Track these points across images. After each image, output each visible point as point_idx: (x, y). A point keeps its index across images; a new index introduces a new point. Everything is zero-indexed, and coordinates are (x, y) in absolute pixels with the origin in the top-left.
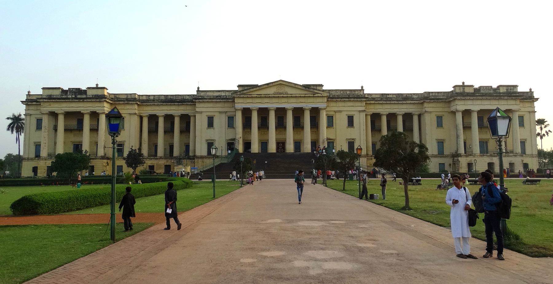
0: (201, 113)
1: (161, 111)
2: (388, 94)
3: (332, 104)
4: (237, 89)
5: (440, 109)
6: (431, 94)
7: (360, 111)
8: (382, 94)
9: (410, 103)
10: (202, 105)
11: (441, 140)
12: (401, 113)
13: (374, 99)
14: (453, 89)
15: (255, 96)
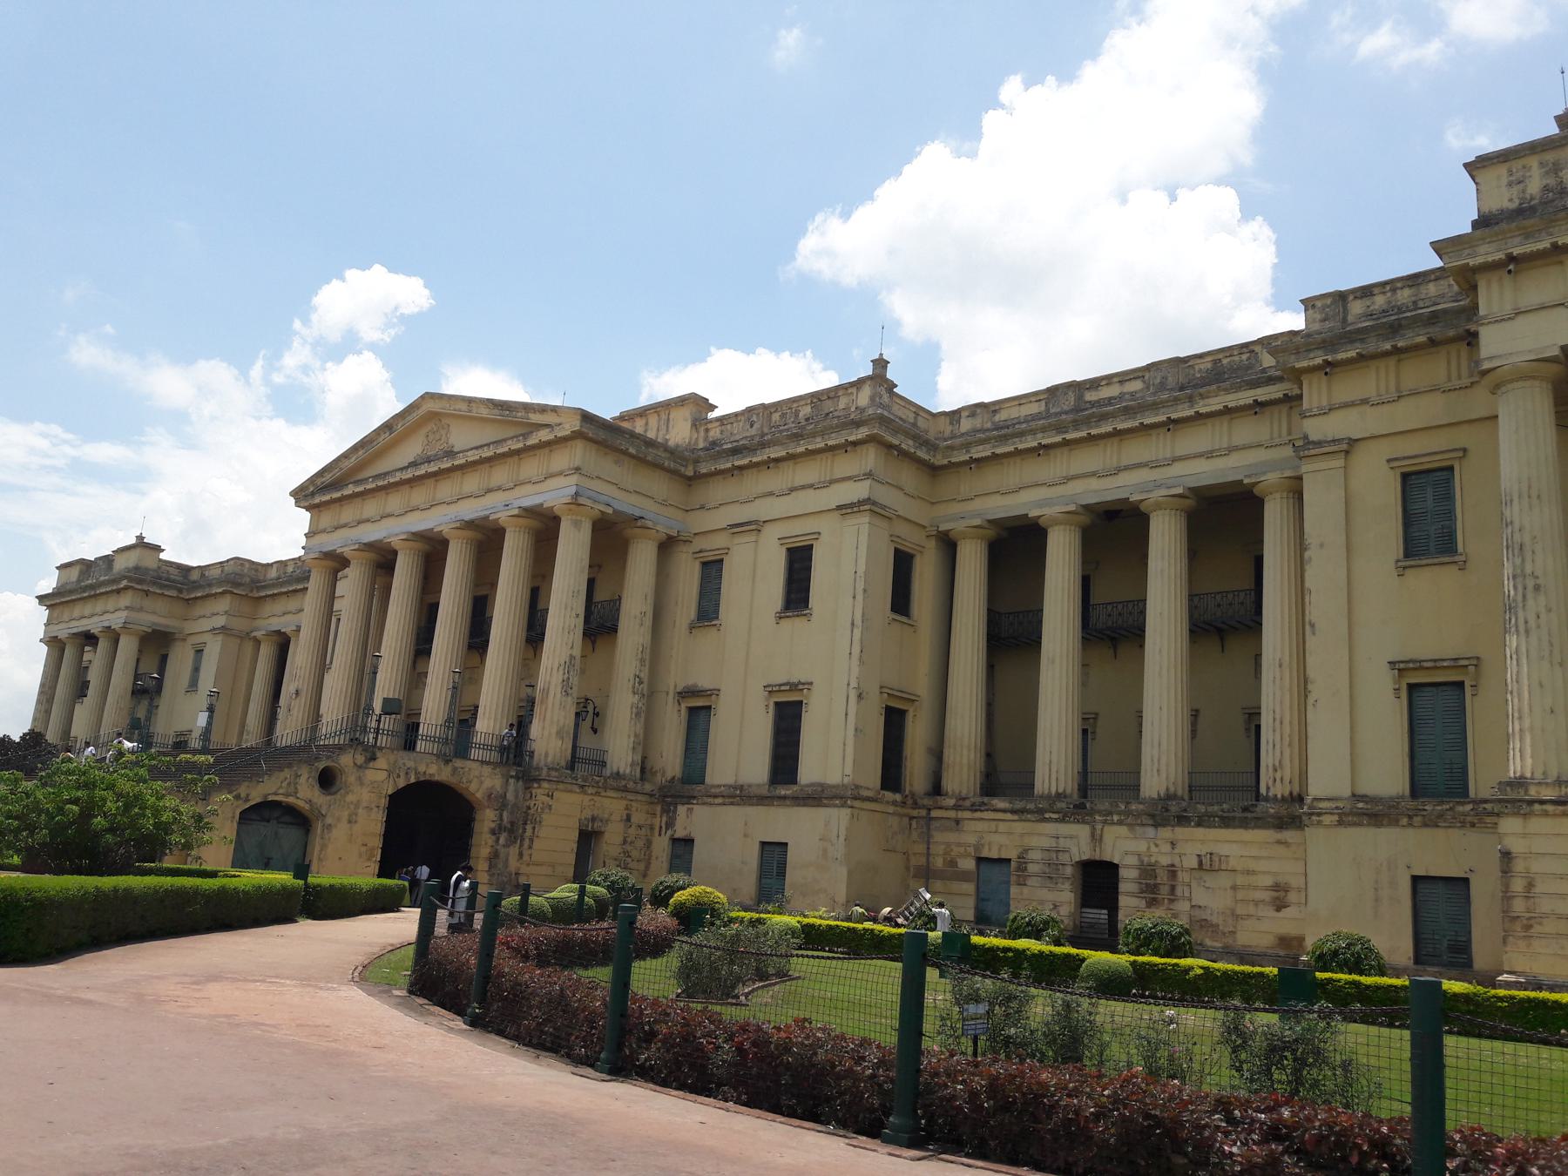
2: (1094, 384)
3: (718, 491)
5: (1429, 409)
6: (1357, 308)
7: (845, 509)
8: (1053, 391)
9: (1227, 411)
11: (1436, 665)
12: (1157, 495)
13: (1007, 431)
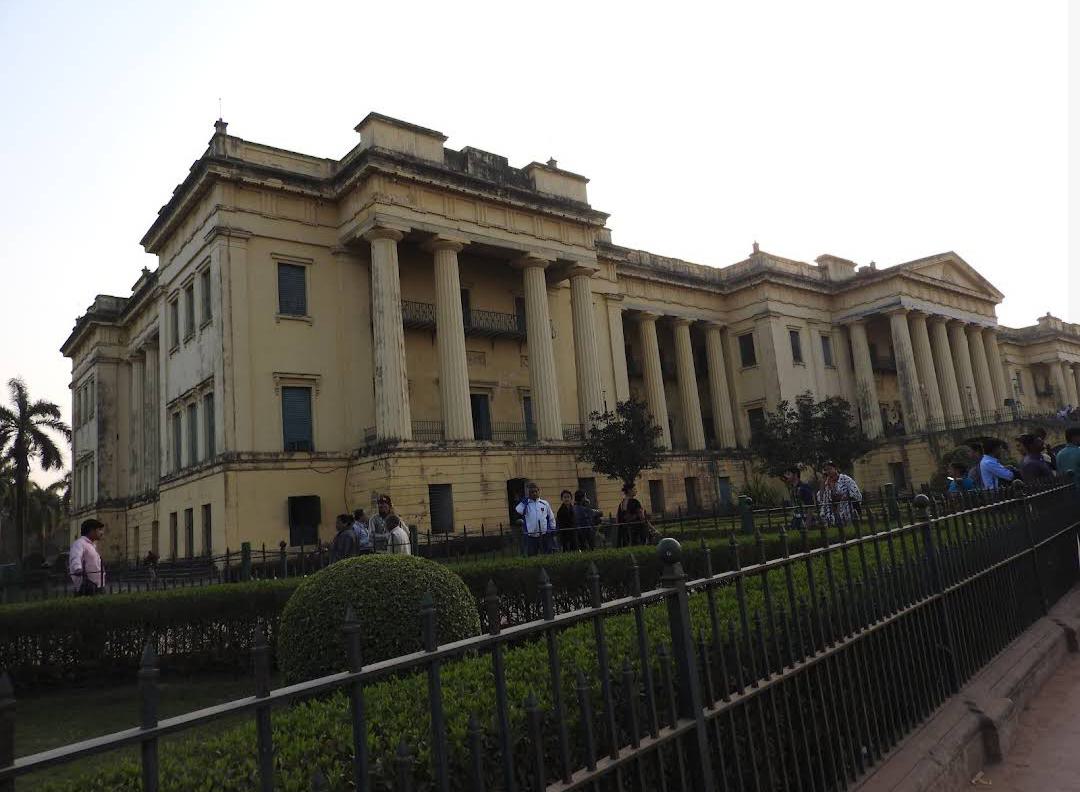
0: (778, 315)
1: (655, 302)
4: (816, 264)
10: (774, 294)
14: (1037, 323)
15: (928, 281)
